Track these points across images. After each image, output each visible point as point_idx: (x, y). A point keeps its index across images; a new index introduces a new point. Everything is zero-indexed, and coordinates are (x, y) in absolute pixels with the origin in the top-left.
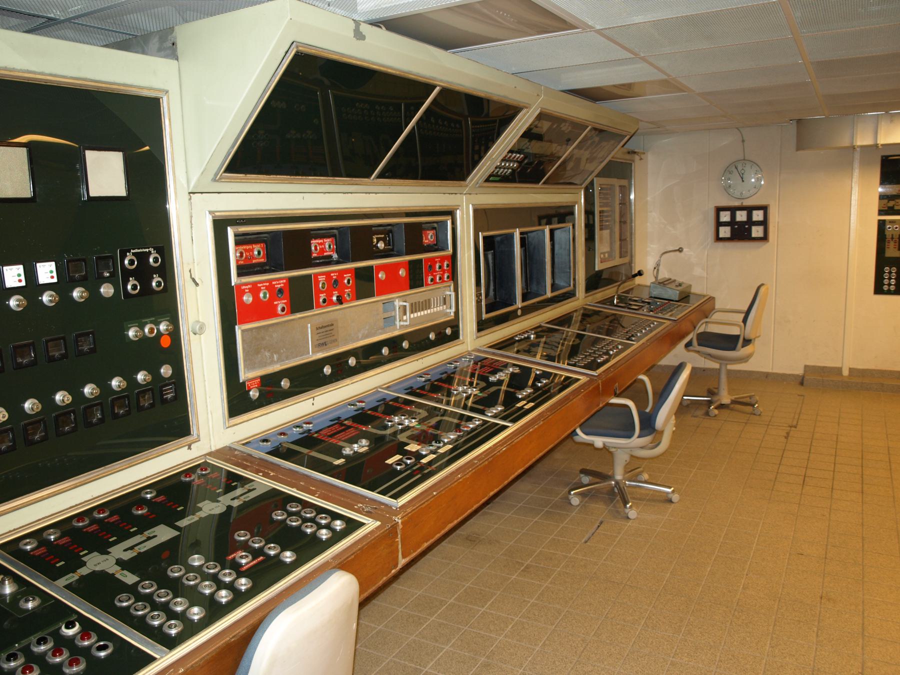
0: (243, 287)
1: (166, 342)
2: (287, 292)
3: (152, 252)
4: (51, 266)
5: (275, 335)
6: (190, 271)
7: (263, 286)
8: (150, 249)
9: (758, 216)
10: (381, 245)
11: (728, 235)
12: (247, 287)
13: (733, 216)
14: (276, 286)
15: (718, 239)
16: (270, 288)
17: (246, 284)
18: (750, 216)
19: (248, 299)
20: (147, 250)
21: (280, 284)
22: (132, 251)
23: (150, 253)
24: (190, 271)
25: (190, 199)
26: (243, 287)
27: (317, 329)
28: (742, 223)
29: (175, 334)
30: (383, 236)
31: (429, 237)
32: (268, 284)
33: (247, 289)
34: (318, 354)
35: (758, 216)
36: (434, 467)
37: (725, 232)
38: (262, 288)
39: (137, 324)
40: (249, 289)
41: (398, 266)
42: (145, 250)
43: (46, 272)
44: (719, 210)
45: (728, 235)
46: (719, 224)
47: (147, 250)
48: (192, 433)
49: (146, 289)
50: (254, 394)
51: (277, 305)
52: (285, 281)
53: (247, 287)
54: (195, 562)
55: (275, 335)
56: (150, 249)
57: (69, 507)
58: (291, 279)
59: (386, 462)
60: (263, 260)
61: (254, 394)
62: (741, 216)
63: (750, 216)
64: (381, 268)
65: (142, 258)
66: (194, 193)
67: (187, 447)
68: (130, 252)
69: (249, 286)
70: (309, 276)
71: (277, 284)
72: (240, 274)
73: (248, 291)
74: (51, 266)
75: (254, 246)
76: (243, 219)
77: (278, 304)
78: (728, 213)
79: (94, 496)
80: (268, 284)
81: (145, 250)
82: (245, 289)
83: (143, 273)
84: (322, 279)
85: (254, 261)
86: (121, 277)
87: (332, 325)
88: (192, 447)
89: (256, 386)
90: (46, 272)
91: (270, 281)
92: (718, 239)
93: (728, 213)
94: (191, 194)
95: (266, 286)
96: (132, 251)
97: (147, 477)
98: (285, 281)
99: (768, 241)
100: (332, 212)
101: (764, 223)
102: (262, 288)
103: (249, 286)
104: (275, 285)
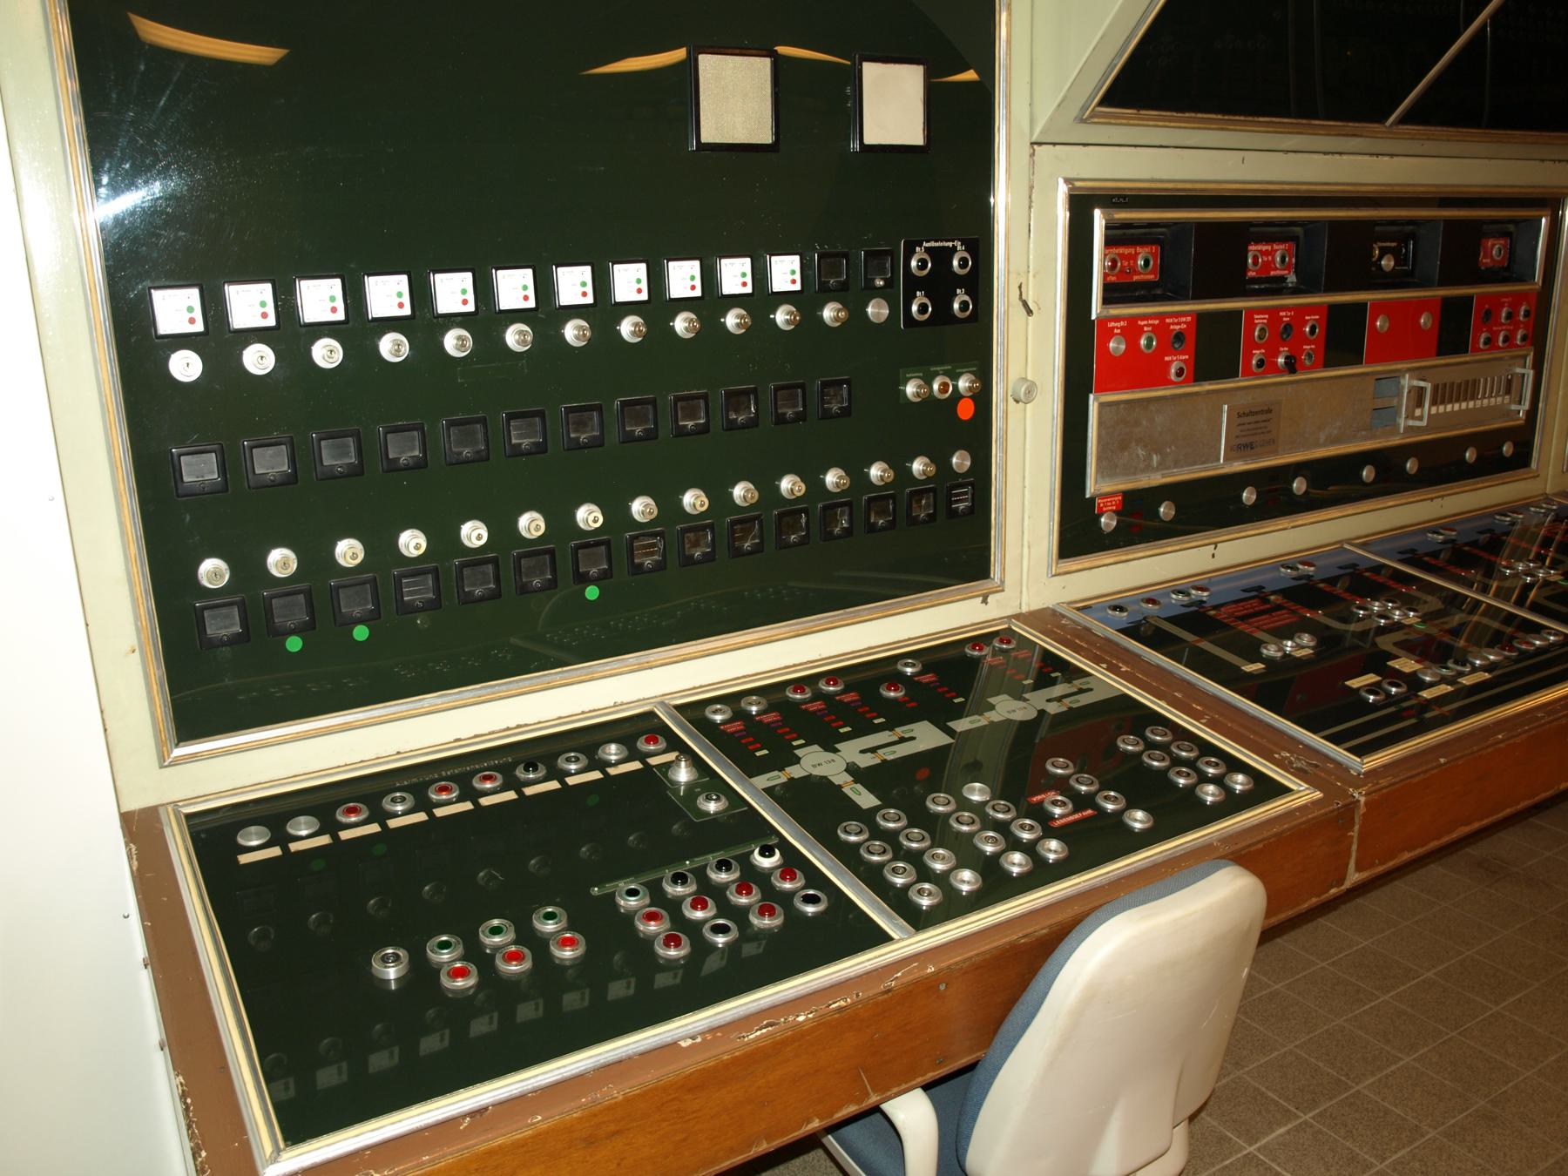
0: (1112, 324)
1: (966, 411)
2: (1191, 341)
3: (959, 248)
4: (793, 262)
5: (1159, 419)
6: (1020, 287)
7: (1148, 325)
8: (955, 243)
10: (1387, 263)
12: (1118, 325)
14: (1172, 327)
16: (1161, 330)
17: (1117, 319)
19: (1116, 346)
20: (950, 244)
22: (925, 244)
23: (954, 249)
24: (1020, 287)
25: (1032, 155)
26: (1112, 324)
27: (1240, 416)
29: (983, 398)
30: (1394, 244)
31: (1494, 250)
32: (1157, 322)
33: (1117, 328)
34: (1236, 464)
38: (1145, 329)
39: (921, 374)
40: (1121, 328)
41: (1422, 305)
42: (946, 244)
43: (785, 272)
47: (950, 244)
48: (992, 576)
49: (942, 313)
50: (1107, 522)
51: (1169, 364)
52: (1189, 319)
53: (1118, 325)
54: (972, 794)
55: (1159, 419)
56: (955, 243)
57: (783, 666)
58: (1201, 317)
59: (1348, 683)
61: (1107, 522)
64: (1380, 308)
65: (941, 257)
66: (1040, 144)
67: (981, 598)
68: (921, 246)
69: (1122, 323)
70: (1237, 314)
71: (1173, 324)
72: (1107, 300)
73: (1119, 331)
74: (793, 262)
75: (1139, 249)
76: (1124, 197)
77: (1172, 361)
79: (824, 656)
80: (1157, 322)
81: (946, 244)
82: (1113, 328)
83: (939, 284)
84: (1261, 320)
85: (1136, 278)
86: (901, 289)
87: (1270, 411)
88: (989, 599)
89: (1114, 508)
90: (785, 272)
94: (1035, 146)
96: (925, 244)
97: (910, 639)
98: (1189, 319)
100: (1298, 191)
102: (1145, 329)
103: (1122, 323)
104: (1170, 324)
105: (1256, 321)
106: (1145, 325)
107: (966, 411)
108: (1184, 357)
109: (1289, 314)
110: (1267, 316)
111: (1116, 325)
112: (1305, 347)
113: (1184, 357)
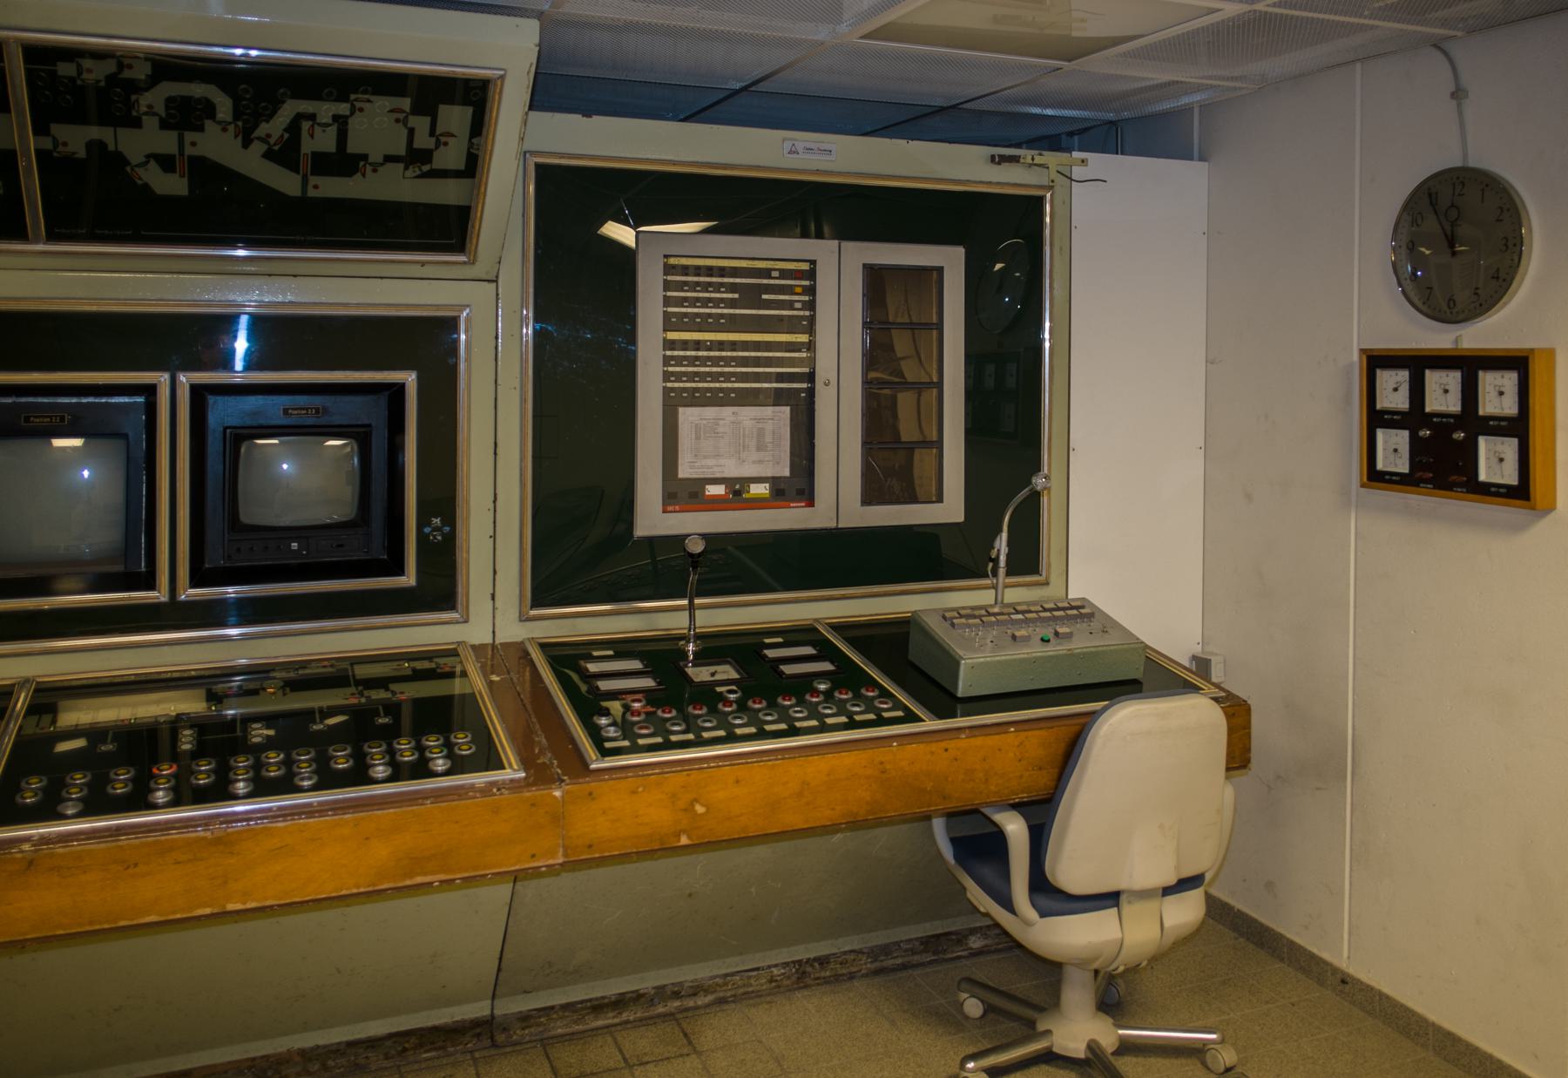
9: (1498, 396)
11: (1403, 467)
13: (1417, 391)
15: (1375, 477)
18: (1470, 393)
28: (1443, 424)
35: (1498, 396)
36: (899, 961)
37: (1394, 449)
44: (1376, 362)
45: (1403, 467)
46: (1377, 419)
62: (1443, 393)
63: (1470, 393)
78: (1453, 379)
92: (1375, 477)
93: (1453, 379)
99: (1551, 507)
101: (1518, 427)
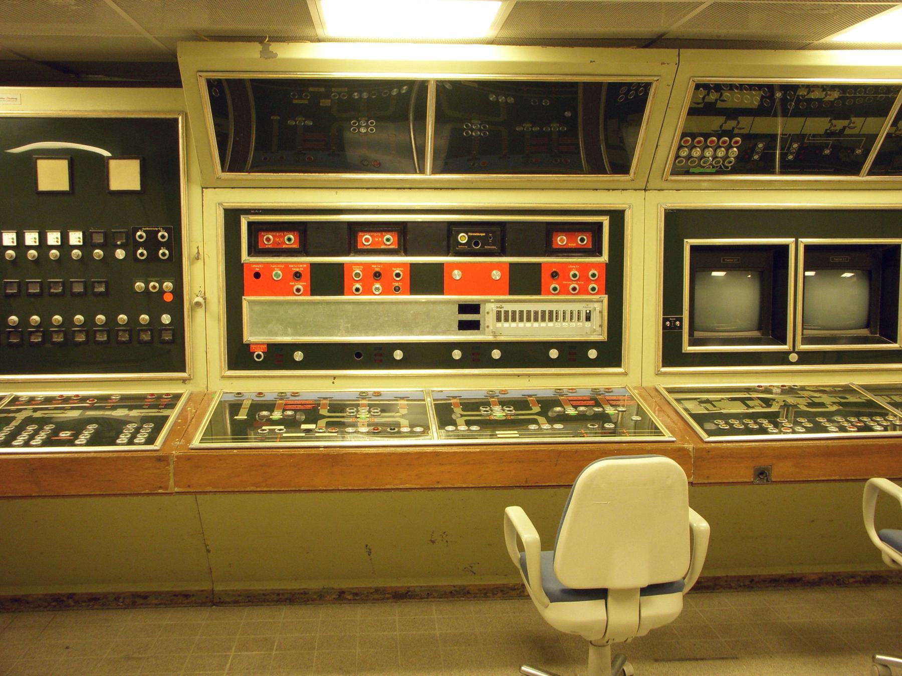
0: (254, 266)
1: (168, 298)
6: (198, 248)
7: (277, 268)
20: (157, 229)
21: (299, 268)
22: (143, 229)
26: (254, 266)
32: (283, 266)
33: (257, 268)
47: (157, 229)
49: (153, 256)
51: (293, 286)
58: (313, 266)
60: (295, 246)
69: (260, 266)
80: (283, 266)
90: (76, 238)
91: (287, 264)
95: (280, 268)
96: (143, 229)
98: (305, 266)
103: (260, 266)
104: (292, 268)
105: (354, 269)
106: (274, 268)
107: (168, 298)
108: (303, 284)
109: (379, 266)
110: (362, 267)
111: (257, 266)
112: (394, 284)
113: (303, 284)
